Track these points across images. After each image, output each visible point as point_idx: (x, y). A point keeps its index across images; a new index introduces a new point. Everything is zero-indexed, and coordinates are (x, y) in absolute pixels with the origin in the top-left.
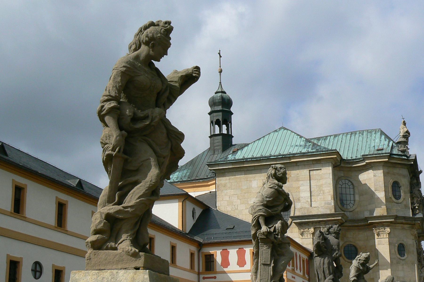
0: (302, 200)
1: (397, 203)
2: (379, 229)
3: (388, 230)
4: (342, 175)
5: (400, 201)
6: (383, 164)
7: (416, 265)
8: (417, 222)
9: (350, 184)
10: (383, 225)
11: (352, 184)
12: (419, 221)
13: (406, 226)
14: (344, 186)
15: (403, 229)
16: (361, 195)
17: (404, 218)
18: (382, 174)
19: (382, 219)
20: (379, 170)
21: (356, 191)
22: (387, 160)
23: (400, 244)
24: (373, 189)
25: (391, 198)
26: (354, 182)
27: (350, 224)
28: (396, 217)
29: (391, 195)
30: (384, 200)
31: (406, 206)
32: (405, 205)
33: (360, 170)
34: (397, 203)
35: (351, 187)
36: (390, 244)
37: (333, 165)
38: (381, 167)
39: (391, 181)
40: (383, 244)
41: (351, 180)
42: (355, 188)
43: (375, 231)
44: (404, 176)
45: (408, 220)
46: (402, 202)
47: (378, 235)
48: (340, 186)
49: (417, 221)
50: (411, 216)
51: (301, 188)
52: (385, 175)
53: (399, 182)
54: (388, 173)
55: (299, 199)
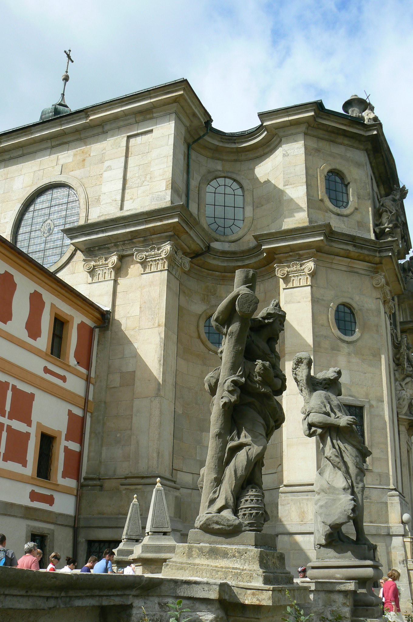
0: (104, 199)
1: (338, 215)
2: (289, 267)
3: (310, 265)
4: (219, 168)
5: (346, 211)
6: (303, 128)
7: (383, 357)
8: (384, 254)
9: (235, 186)
10: (296, 254)
11: (242, 187)
12: (391, 250)
13: (360, 265)
14: (221, 190)
15: (352, 271)
16: (256, 205)
17: (353, 240)
18: (302, 150)
19: (294, 239)
20: (296, 141)
21: (249, 199)
22: (312, 113)
23: (344, 305)
24: (281, 186)
25: (322, 200)
26: (245, 183)
27: (225, 264)
28: (330, 234)
29: (321, 193)
30: (303, 204)
31: (361, 225)
32: (358, 222)
33: (257, 157)
34: (338, 215)
35: (239, 192)
36: (315, 301)
37: (188, 131)
38: (301, 136)
39: (324, 167)
40: (297, 303)
41: (238, 178)
42: (246, 193)
43: (279, 273)
44: (358, 165)
45: (362, 248)
46: (352, 214)
47: (286, 279)
48: (213, 190)
49: (386, 250)
50: (373, 237)
51: (105, 175)
52: (308, 152)
53: (345, 172)
54: (318, 150)
55: (98, 200)
